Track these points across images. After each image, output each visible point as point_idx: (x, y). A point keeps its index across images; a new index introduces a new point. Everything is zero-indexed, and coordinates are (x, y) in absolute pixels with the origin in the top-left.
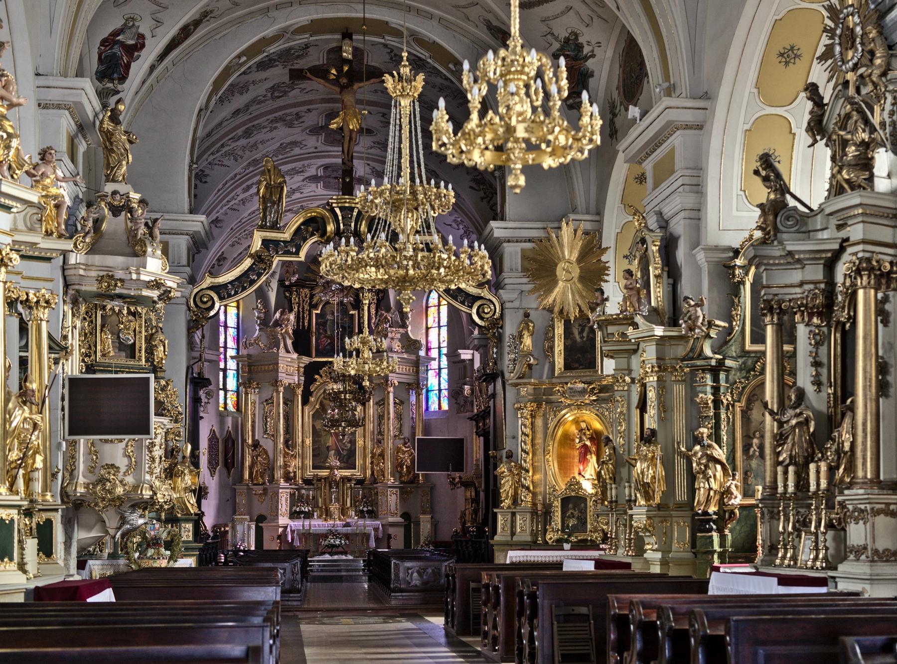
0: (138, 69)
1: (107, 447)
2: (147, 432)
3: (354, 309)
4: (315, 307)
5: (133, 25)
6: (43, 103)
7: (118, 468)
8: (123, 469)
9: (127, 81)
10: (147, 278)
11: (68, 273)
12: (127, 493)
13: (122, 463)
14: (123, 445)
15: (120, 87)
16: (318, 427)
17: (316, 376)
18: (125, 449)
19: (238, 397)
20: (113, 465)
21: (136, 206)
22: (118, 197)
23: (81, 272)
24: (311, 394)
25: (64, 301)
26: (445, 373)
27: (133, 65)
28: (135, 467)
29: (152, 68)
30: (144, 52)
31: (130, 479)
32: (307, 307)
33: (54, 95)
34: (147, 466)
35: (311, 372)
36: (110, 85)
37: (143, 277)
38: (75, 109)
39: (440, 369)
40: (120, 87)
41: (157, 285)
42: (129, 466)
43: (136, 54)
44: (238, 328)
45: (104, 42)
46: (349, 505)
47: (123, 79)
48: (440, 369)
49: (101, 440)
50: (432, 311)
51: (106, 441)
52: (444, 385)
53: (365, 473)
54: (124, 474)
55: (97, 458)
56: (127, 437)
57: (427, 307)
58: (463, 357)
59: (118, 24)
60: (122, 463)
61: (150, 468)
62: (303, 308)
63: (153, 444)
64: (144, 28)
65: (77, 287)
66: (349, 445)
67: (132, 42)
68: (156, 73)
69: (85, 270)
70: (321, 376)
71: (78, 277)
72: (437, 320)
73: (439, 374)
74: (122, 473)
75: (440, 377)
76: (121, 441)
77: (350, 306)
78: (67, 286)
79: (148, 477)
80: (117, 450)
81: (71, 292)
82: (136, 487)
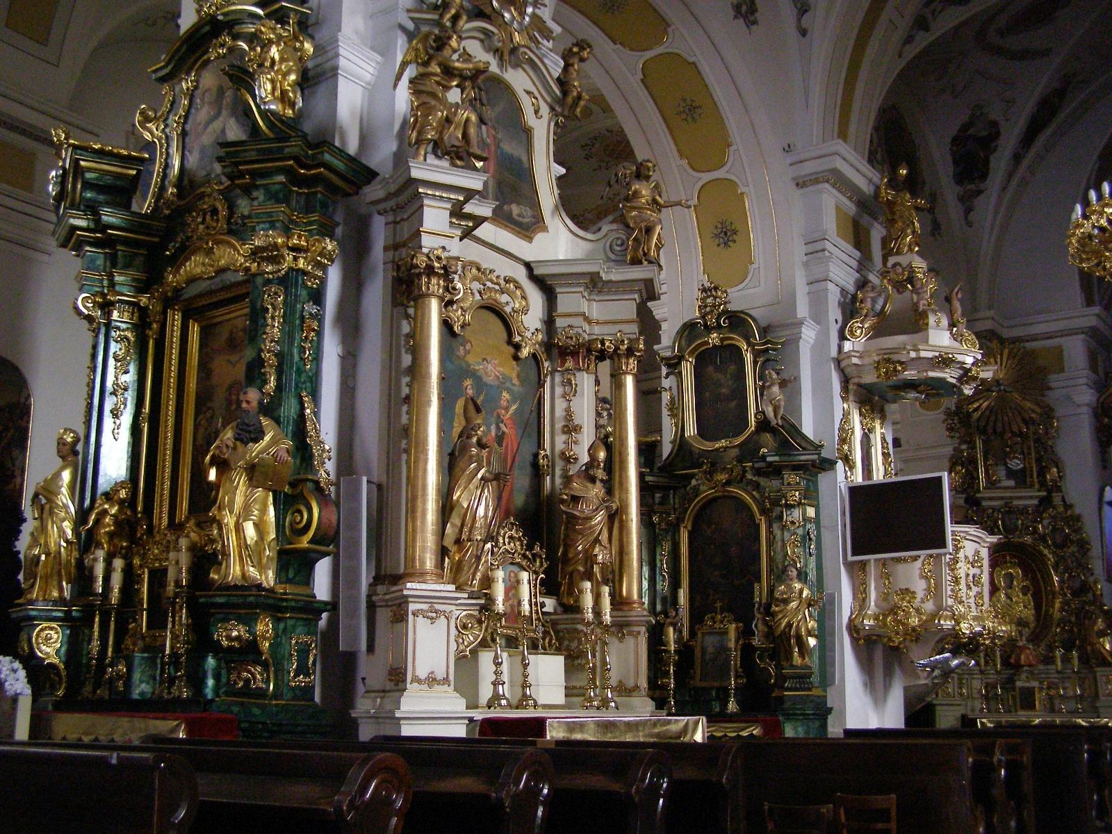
0: (1000, 162)
1: (900, 568)
2: (943, 545)
5: (982, 114)
6: (801, 181)
7: (914, 593)
8: (920, 594)
9: (989, 178)
10: (930, 355)
11: (843, 364)
12: (923, 624)
13: (919, 587)
14: (918, 564)
15: (982, 186)
18: (922, 569)
20: (907, 589)
21: (920, 276)
22: (899, 270)
23: (855, 360)
25: (844, 399)
27: (991, 158)
28: (935, 591)
29: (1017, 158)
30: (1001, 141)
31: (929, 606)
33: (809, 168)
34: (949, 588)
36: (972, 187)
37: (923, 354)
38: (839, 181)
40: (982, 186)
41: (944, 361)
42: (928, 589)
43: (993, 145)
45: (955, 141)
47: (984, 176)
49: (892, 559)
51: (899, 560)
54: (922, 601)
55: (889, 583)
56: (923, 553)
59: (965, 118)
60: (919, 587)
61: (952, 590)
63: (955, 561)
64: (995, 114)
65: (856, 380)
67: (984, 133)
68: (1026, 162)
69: (860, 357)
71: (854, 368)
74: (918, 599)
76: (915, 558)
78: (845, 381)
79: (950, 602)
80: (912, 571)
81: (851, 387)
82: (934, 615)
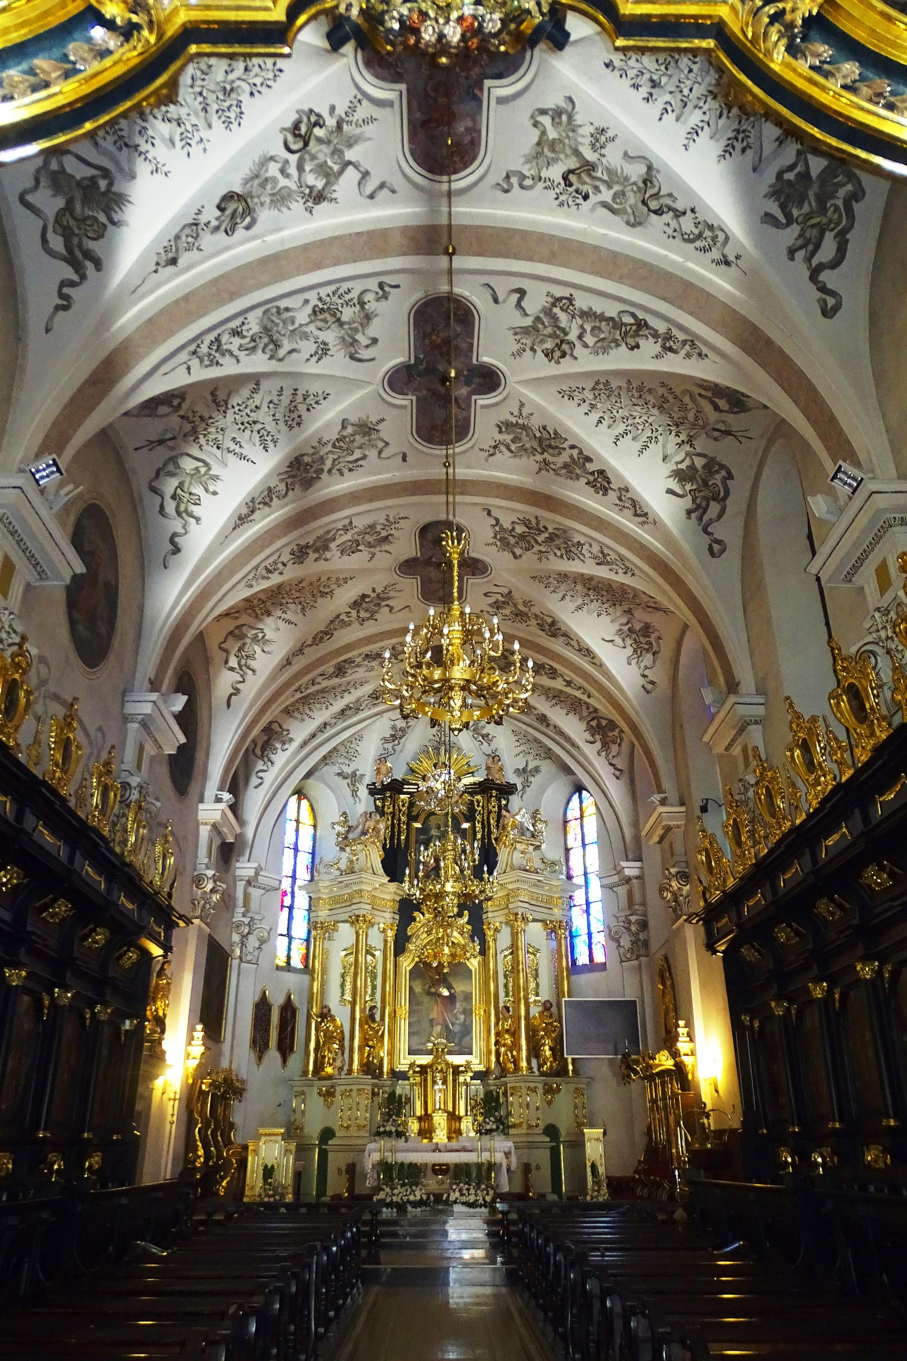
3: (467, 821)
4: (416, 819)
16: (418, 989)
17: (416, 914)
19: (308, 949)
24: (408, 939)
26: (597, 910)
32: (403, 819)
35: (407, 909)
39: (588, 904)
44: (313, 854)
46: (462, 1113)
48: (588, 904)
50: (574, 827)
52: (597, 925)
53: (489, 1060)
57: (566, 822)
58: (627, 872)
62: (399, 820)
66: (462, 1017)
70: (423, 914)
72: (579, 837)
73: (587, 911)
75: (588, 915)
77: (461, 818)
